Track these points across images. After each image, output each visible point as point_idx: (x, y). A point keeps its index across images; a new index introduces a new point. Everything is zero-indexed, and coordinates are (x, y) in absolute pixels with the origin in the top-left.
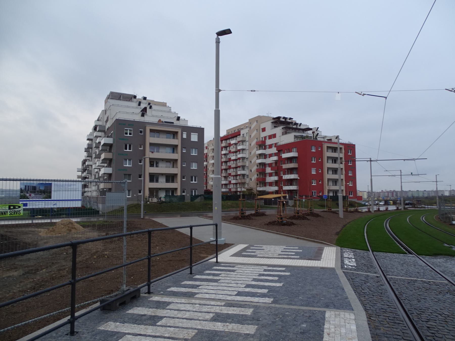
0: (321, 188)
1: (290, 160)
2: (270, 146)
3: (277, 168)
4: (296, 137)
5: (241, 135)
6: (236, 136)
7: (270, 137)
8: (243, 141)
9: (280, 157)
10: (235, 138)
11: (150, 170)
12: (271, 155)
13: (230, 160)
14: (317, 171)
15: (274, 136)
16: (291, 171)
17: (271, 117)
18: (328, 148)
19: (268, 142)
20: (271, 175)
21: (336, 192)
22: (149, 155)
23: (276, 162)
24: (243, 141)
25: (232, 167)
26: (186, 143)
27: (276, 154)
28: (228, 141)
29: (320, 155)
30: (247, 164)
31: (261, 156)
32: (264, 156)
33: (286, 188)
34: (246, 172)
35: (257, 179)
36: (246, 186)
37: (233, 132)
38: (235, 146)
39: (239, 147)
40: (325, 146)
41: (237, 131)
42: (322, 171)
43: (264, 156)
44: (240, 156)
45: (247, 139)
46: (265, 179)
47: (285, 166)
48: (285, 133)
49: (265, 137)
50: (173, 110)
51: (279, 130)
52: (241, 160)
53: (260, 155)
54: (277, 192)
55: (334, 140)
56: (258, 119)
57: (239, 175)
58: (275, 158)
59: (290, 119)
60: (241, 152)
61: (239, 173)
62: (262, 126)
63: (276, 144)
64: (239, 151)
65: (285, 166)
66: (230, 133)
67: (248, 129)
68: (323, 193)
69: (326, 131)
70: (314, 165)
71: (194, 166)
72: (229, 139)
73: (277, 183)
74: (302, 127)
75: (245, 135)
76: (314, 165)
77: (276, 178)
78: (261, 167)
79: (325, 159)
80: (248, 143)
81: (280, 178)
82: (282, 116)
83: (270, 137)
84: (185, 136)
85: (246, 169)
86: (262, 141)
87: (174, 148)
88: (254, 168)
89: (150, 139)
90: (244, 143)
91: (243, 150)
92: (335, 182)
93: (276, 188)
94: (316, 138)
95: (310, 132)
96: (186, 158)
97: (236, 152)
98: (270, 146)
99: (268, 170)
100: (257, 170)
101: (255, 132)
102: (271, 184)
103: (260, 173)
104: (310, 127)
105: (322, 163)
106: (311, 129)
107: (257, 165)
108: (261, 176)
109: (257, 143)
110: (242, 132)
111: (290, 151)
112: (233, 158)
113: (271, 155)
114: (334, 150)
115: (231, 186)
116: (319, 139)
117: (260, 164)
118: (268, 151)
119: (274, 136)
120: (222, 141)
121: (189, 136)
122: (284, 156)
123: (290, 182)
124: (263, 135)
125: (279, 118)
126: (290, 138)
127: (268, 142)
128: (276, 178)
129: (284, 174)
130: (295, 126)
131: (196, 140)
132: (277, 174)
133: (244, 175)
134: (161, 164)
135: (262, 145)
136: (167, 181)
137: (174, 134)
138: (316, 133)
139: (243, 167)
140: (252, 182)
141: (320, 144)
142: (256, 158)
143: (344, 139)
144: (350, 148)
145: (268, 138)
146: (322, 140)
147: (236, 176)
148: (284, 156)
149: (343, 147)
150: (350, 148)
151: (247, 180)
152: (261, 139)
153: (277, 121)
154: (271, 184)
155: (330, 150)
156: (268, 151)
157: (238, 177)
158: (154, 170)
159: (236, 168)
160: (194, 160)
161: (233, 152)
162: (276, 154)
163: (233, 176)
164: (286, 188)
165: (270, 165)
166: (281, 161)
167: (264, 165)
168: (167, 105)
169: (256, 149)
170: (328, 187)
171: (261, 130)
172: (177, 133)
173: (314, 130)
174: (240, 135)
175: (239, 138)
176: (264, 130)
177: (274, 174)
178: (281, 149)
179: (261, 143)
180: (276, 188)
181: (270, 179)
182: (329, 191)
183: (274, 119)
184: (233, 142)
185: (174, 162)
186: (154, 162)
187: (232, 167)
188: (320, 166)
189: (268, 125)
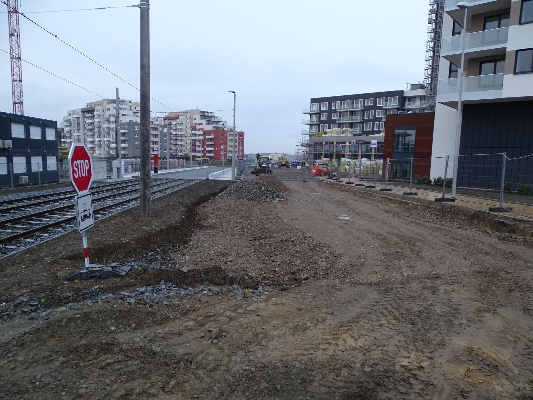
1: (210, 140)
2: (199, 130)
3: (203, 143)
4: (214, 127)
5: (180, 120)
7: (199, 124)
15: (201, 124)
16: (210, 146)
20: (199, 146)
27: (202, 135)
28: (170, 121)
29: (225, 138)
30: (184, 138)
31: (193, 135)
33: (207, 155)
34: (183, 143)
40: (228, 133)
41: (176, 115)
43: (196, 135)
44: (179, 133)
45: (184, 122)
48: (208, 124)
49: (196, 124)
51: (204, 122)
56: (191, 112)
58: (202, 138)
62: (194, 116)
63: (202, 129)
66: (171, 116)
67: (184, 116)
73: (203, 151)
74: (216, 120)
76: (222, 144)
77: (202, 149)
80: (184, 126)
81: (205, 149)
82: (206, 111)
83: (199, 124)
88: (189, 142)
91: (181, 129)
95: (222, 123)
96: (162, 141)
98: (199, 130)
99: (198, 143)
102: (199, 152)
105: (226, 142)
109: (191, 127)
110: (180, 117)
113: (199, 135)
115: (172, 151)
116: (226, 129)
118: (198, 132)
119: (201, 124)
120: (164, 120)
121: (163, 129)
122: (208, 137)
123: (210, 152)
124: (195, 122)
125: (204, 112)
126: (210, 128)
127: (198, 127)
128: (202, 149)
129: (207, 147)
130: (213, 119)
132: (203, 146)
133: (181, 145)
135: (194, 128)
139: (181, 140)
140: (187, 149)
141: (225, 133)
142: (189, 136)
144: (242, 134)
147: (176, 145)
148: (208, 137)
150: (242, 134)
151: (184, 149)
153: (205, 115)
154: (199, 152)
155: (231, 136)
156: (198, 132)
157: (177, 146)
159: (176, 140)
162: (202, 135)
164: (207, 155)
165: (199, 141)
166: (204, 140)
167: (195, 140)
170: (229, 155)
172: (157, 128)
175: (179, 121)
176: (195, 119)
178: (206, 133)
184: (174, 122)
188: (225, 144)
189: (198, 117)
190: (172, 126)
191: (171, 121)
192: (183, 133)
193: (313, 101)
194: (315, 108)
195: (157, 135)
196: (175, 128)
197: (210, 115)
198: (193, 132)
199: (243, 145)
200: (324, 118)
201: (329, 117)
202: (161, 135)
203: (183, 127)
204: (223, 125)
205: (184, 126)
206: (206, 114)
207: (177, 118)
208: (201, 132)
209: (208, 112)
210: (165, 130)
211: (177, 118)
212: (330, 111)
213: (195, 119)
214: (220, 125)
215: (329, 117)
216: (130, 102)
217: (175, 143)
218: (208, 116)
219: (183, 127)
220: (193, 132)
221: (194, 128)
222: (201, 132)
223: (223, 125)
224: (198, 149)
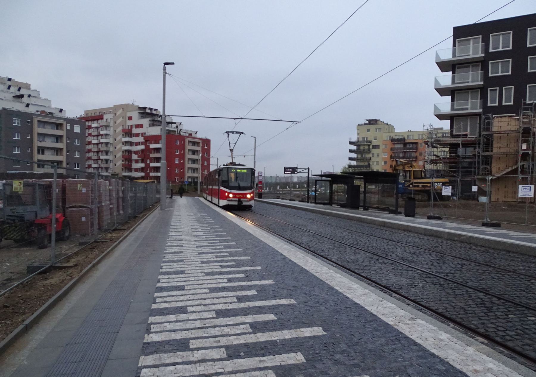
0: (182, 175)
2: (137, 135)
3: (144, 155)
5: (105, 120)
6: (98, 120)
7: (137, 126)
8: (107, 127)
9: (147, 148)
10: (96, 122)
11: (38, 157)
12: (137, 144)
13: (90, 143)
14: (180, 161)
15: (141, 126)
17: (135, 106)
18: (189, 142)
19: (135, 131)
20: (137, 162)
21: (193, 178)
22: (37, 143)
23: (143, 151)
24: (107, 127)
25: (93, 150)
26: (70, 134)
27: (142, 143)
29: (182, 147)
30: (111, 149)
31: (126, 143)
32: (131, 144)
33: (152, 174)
34: (110, 157)
35: (123, 165)
36: (110, 171)
37: (93, 115)
38: (96, 130)
39: (102, 132)
40: (187, 140)
41: (97, 114)
42: (184, 161)
43: (131, 144)
44: (102, 141)
45: (111, 124)
46: (131, 165)
47: (152, 155)
49: (132, 126)
50: (42, 96)
51: (146, 122)
52: (104, 145)
53: (126, 142)
54: (142, 178)
55: (193, 135)
56: (125, 107)
57: (102, 160)
58: (143, 147)
59: (155, 110)
60: (104, 137)
61: (102, 157)
62: (129, 114)
63: (142, 134)
64: (102, 135)
65: (152, 155)
66: (89, 115)
67: (113, 115)
68: (184, 179)
69: (188, 126)
70: (177, 156)
71: (77, 155)
72: (89, 121)
73: (142, 170)
75: (109, 120)
76: (177, 156)
77: (143, 165)
78: (127, 154)
79: (187, 151)
80: (112, 129)
81: (147, 166)
82: (148, 106)
83: (137, 126)
84: (68, 128)
85: (109, 154)
86: (128, 129)
87: (58, 138)
88: (120, 154)
89: (38, 130)
90: (108, 128)
91: (106, 135)
92: (194, 170)
93: (143, 174)
94: (180, 134)
95: (174, 125)
96: (70, 148)
97: (97, 136)
98: (137, 135)
99: (135, 157)
100: (123, 156)
101: (121, 119)
102: (137, 170)
103: (126, 159)
104: (173, 121)
106: (175, 123)
107: (123, 152)
108: (127, 163)
109: (123, 130)
110: (105, 117)
111: (157, 142)
112: (95, 141)
113: (137, 144)
114: (194, 144)
116: (182, 134)
117: (126, 150)
118: (134, 140)
119: (141, 126)
122: (152, 146)
124: (129, 123)
125: (145, 108)
126: (155, 131)
127: (135, 131)
128: (143, 165)
129: (151, 162)
131: (79, 132)
133: (107, 160)
134: (46, 152)
135: (128, 133)
136: (39, 166)
137: (58, 126)
138: (179, 128)
139: (107, 153)
141: (182, 139)
142: (121, 144)
143: (201, 135)
144: (206, 142)
145: (134, 127)
146: (184, 134)
148: (152, 146)
149: (201, 141)
150: (206, 142)
151: (111, 165)
152: (127, 128)
153: (144, 112)
154: (137, 170)
155: (191, 144)
156: (134, 140)
157: (100, 162)
158: (41, 157)
159: (98, 152)
160: (77, 149)
161: (94, 136)
162: (142, 143)
163: (94, 160)
164: (152, 174)
165: (136, 152)
166: (147, 150)
167: (130, 152)
168: (32, 88)
169: (121, 135)
171: (127, 118)
172: (61, 125)
173: (178, 125)
174: (103, 119)
175: (102, 122)
176: (130, 118)
177: (140, 161)
178: (148, 139)
179: (127, 131)
180: (143, 174)
181: (134, 166)
182: (189, 177)
183: (140, 108)
184: (94, 125)
185: (58, 151)
186: (41, 150)
187: (93, 150)
189: (135, 115)
190: (91, 131)
191: (90, 123)
192: (110, 140)
193: (461, 33)
194: (474, 49)
195: (61, 137)
196: (96, 133)
197: (154, 112)
198: (127, 139)
199: (208, 160)
200: (501, 69)
201: (519, 66)
202: (68, 138)
203: (110, 131)
204: (177, 127)
205: (112, 129)
206: (149, 111)
207: (100, 117)
208: (141, 139)
209: (151, 109)
210: (77, 129)
211: (100, 117)
212: (519, 53)
213: (130, 118)
214: (172, 127)
215: (519, 66)
216: (10, 80)
217: (96, 158)
218: (151, 115)
219: (110, 131)
220: (127, 139)
221: (128, 133)
222: (141, 139)
223: (177, 127)
224: (134, 166)
